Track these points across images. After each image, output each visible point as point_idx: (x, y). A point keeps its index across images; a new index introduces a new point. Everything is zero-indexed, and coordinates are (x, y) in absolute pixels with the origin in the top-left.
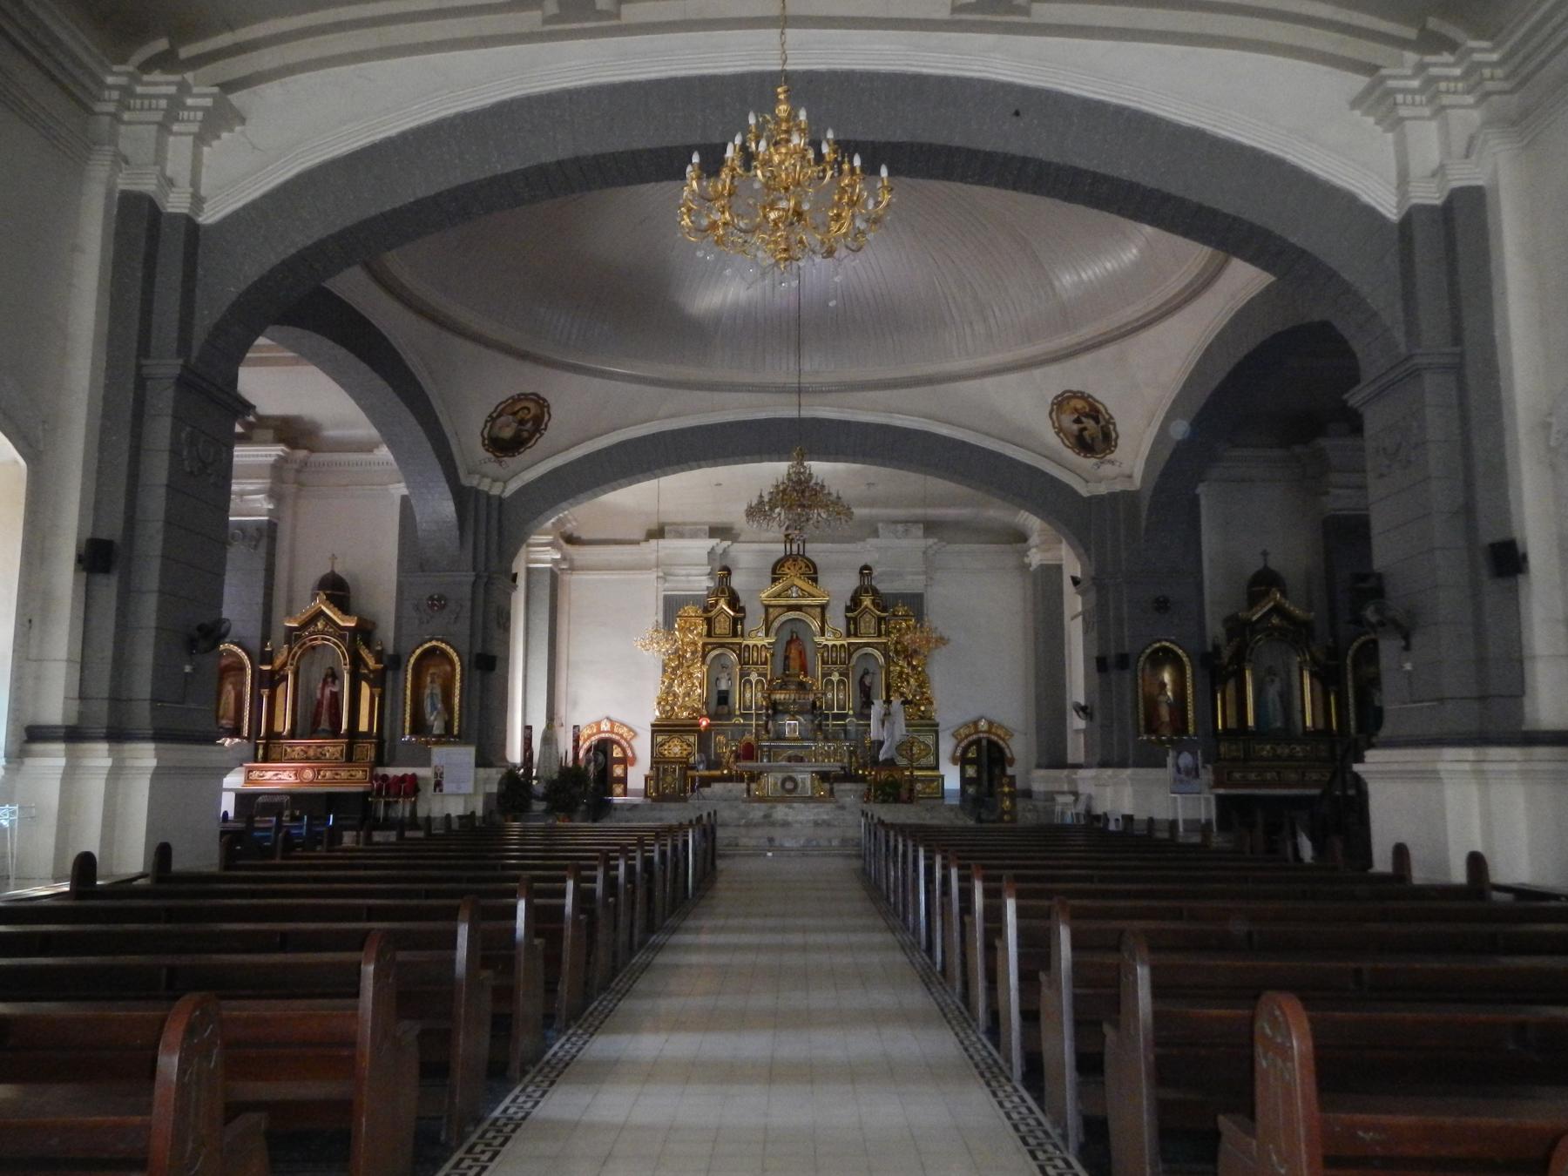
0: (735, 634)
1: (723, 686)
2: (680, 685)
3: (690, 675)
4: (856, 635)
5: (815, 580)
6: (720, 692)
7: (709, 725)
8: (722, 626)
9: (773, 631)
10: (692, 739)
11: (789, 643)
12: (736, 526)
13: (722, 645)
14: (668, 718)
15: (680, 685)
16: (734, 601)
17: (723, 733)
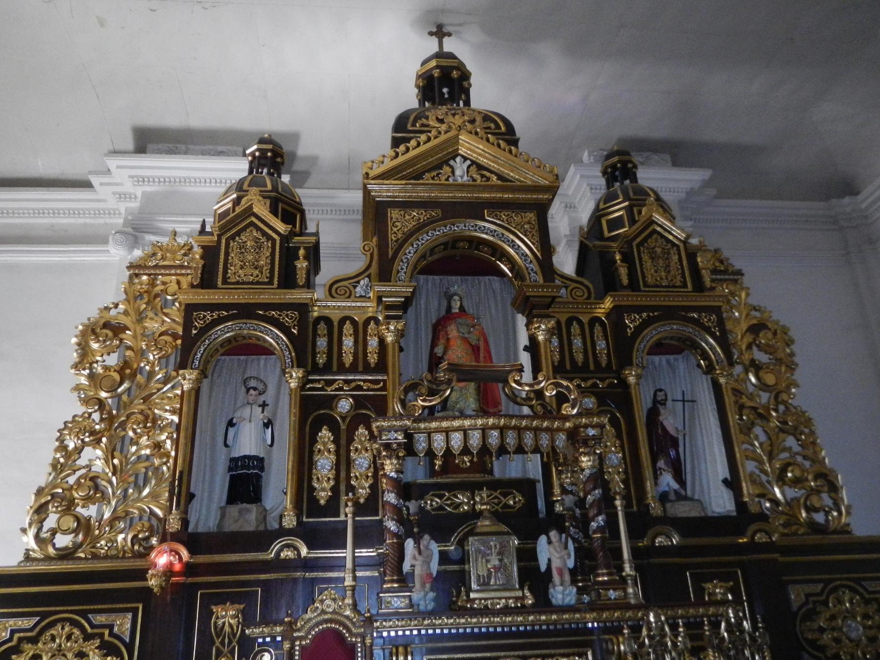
0: (288, 280)
1: (248, 441)
2: (110, 454)
3: (151, 422)
4: (633, 285)
5: (515, 142)
6: (233, 460)
7: (189, 569)
8: (248, 262)
9: (402, 268)
10: (123, 624)
11: (438, 328)
12: (302, 151)
13: (246, 311)
14: (66, 555)
15: (89, 437)
16: (289, 209)
17: (234, 599)
